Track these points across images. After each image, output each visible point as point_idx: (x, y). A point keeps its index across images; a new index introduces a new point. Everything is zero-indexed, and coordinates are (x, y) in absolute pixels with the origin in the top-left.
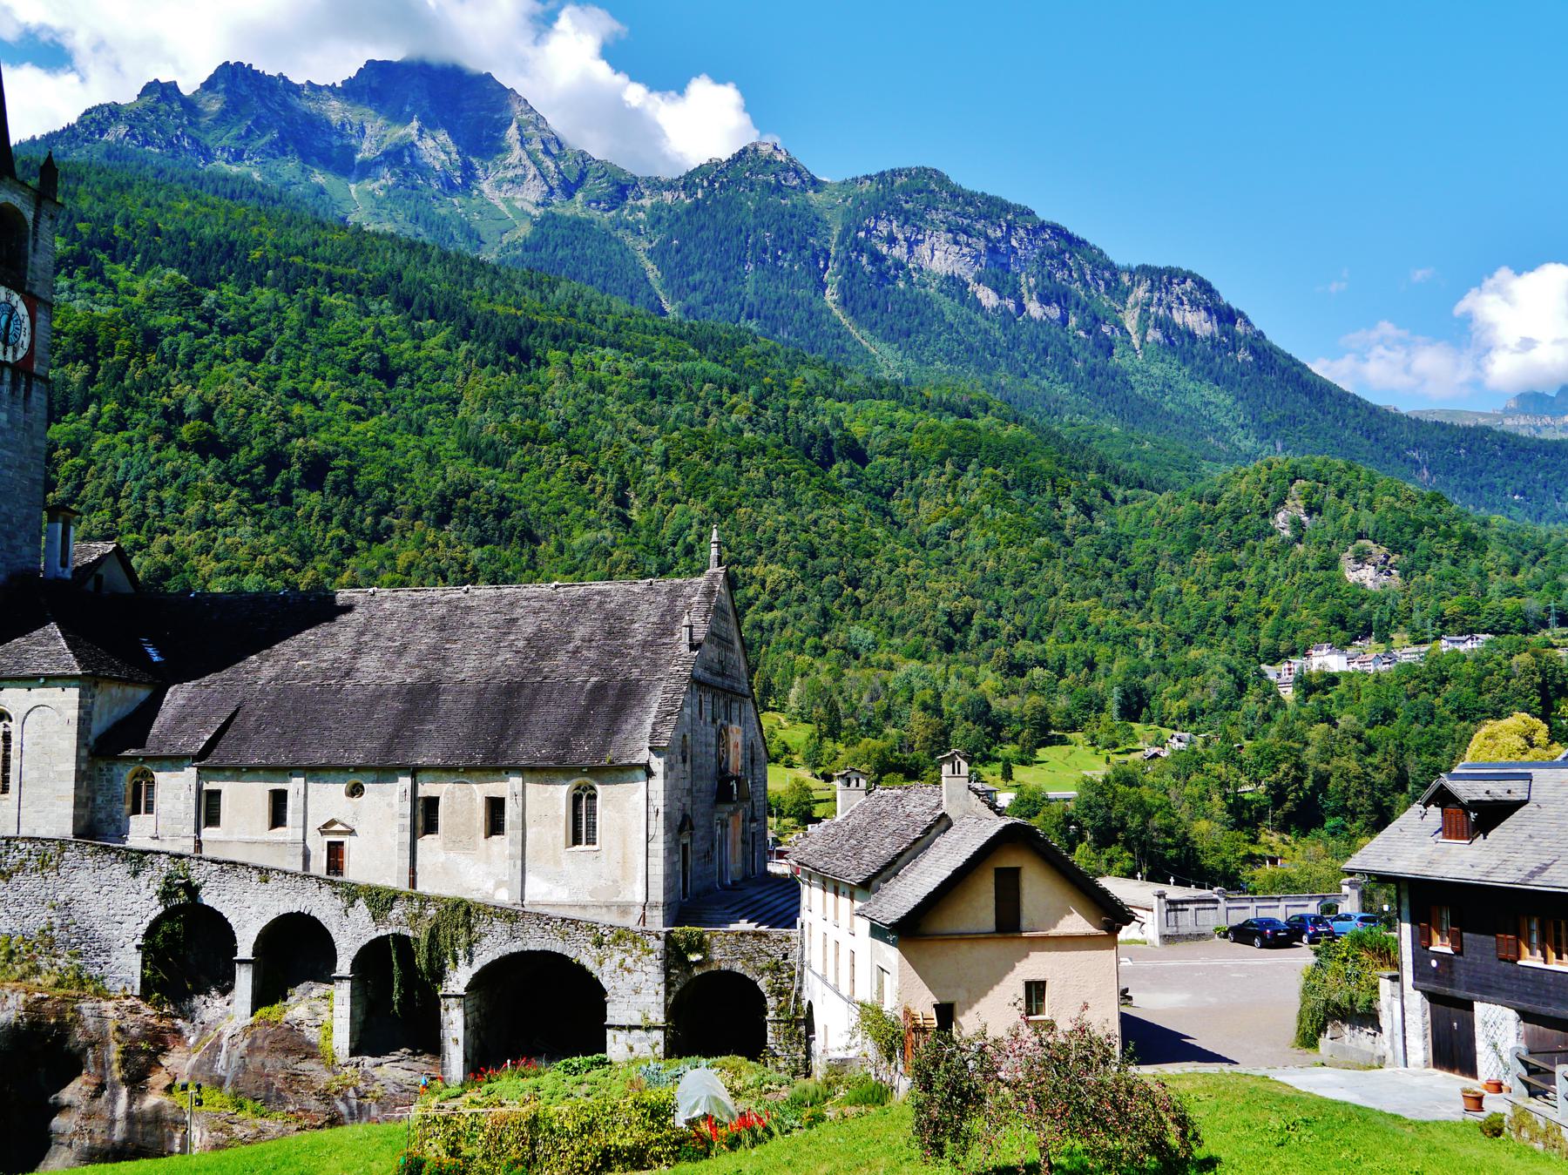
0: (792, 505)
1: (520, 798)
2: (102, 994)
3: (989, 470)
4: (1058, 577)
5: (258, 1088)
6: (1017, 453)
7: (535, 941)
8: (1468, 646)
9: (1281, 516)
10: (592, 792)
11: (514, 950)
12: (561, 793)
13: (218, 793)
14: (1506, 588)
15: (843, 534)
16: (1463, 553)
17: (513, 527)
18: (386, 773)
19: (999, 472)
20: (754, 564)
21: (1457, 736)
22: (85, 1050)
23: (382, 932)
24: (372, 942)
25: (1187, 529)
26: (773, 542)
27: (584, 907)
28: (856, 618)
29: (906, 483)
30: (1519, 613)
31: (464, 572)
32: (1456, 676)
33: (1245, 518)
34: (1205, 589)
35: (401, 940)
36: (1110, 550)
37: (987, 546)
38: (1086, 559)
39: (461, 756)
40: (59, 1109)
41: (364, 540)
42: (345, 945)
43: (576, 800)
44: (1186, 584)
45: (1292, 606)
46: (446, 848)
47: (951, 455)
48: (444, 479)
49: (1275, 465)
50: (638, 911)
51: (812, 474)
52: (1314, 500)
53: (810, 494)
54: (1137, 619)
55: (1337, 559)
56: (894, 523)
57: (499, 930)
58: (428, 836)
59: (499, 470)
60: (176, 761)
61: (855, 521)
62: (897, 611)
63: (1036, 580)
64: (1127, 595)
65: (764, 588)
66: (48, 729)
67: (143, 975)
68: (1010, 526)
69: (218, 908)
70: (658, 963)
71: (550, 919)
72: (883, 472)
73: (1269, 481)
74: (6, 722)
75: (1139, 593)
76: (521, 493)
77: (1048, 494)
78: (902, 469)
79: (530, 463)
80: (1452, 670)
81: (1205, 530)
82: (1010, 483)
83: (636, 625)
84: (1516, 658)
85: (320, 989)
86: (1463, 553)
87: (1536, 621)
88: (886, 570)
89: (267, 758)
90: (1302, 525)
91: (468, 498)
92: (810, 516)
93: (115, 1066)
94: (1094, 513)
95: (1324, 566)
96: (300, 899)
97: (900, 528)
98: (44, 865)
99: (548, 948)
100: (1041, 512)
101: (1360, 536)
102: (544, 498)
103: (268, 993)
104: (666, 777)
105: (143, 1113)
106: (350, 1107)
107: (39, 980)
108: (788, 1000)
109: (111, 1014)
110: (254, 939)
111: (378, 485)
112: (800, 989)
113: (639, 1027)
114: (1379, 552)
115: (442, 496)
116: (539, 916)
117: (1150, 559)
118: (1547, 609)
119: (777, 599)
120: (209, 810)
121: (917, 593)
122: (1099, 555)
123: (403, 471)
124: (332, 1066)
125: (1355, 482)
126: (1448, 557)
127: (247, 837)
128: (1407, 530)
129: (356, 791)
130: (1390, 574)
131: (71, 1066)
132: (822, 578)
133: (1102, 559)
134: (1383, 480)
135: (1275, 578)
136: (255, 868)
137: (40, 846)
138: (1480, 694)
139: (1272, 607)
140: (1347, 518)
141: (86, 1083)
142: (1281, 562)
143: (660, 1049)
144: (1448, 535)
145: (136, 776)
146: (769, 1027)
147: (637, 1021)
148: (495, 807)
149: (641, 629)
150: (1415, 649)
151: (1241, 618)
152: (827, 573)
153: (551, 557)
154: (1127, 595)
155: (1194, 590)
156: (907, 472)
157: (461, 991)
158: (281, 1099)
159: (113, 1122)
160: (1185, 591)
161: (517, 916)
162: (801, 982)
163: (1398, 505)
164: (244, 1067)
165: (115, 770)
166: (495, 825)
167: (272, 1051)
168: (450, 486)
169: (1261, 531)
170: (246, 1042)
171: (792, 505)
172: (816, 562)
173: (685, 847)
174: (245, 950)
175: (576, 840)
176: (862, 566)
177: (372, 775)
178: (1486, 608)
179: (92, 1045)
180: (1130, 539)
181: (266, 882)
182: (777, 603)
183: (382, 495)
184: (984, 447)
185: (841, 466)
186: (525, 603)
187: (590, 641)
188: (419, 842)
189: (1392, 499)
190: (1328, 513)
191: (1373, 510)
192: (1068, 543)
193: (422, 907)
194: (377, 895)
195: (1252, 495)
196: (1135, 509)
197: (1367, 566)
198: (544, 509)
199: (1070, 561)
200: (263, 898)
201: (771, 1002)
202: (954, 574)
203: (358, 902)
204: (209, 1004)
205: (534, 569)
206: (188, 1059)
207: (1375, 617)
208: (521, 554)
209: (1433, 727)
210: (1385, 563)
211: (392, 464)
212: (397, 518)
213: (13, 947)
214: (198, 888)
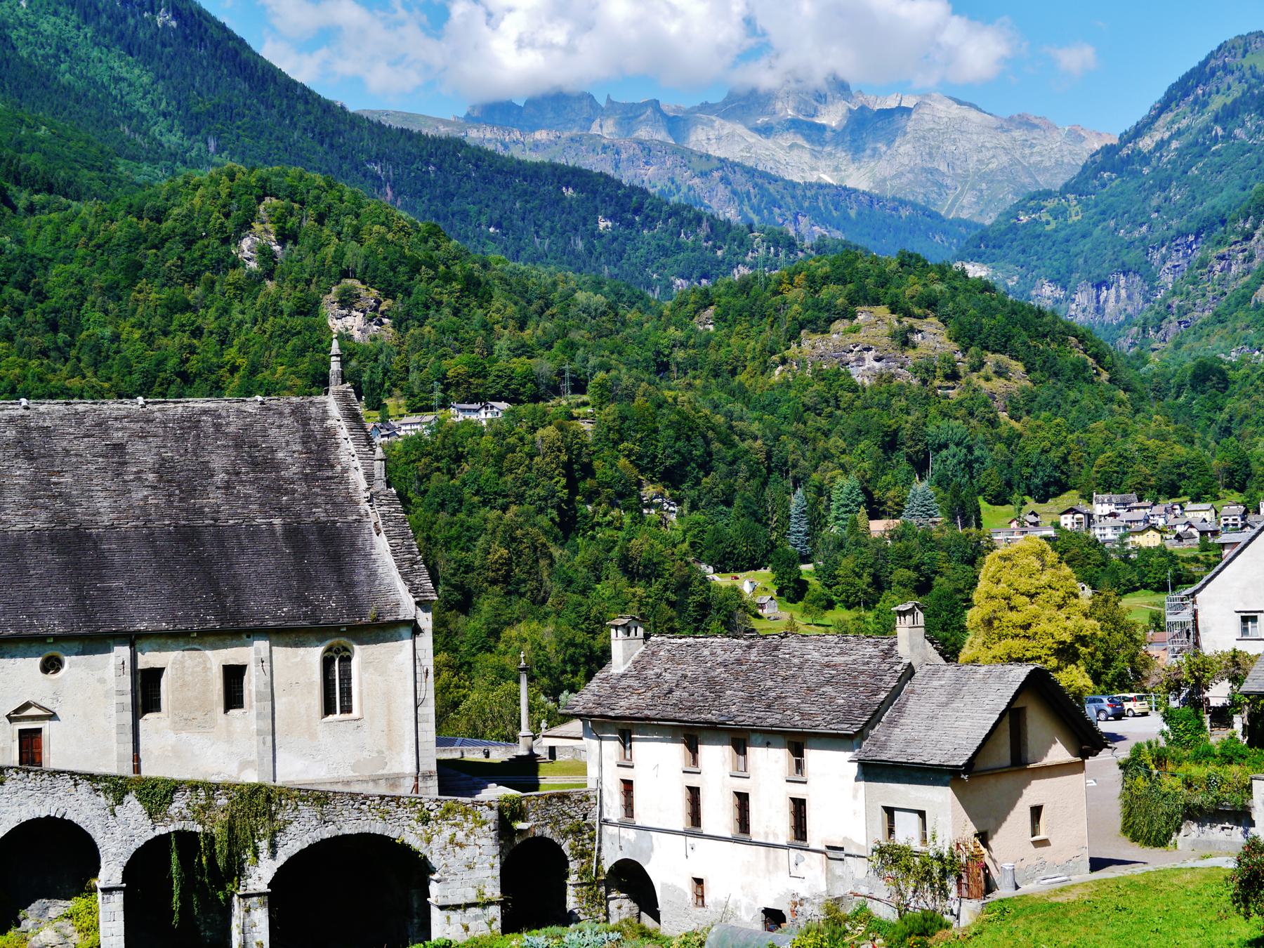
1: (267, 665)
7: (351, 825)
9: (246, 243)
10: (345, 654)
11: (327, 836)
12: (313, 655)
14: (514, 346)
16: (466, 301)
18: (95, 642)
23: (161, 830)
24: (148, 843)
25: (123, 254)
27: (348, 783)
30: (530, 377)
32: (472, 453)
33: (200, 243)
34: (151, 334)
36: (18, 276)
42: (114, 850)
43: (327, 663)
44: (125, 327)
46: (176, 729)
49: (239, 175)
50: (410, 782)
52: (289, 225)
54: (65, 373)
55: (317, 303)
57: (307, 815)
58: (148, 716)
64: (45, 340)
70: (492, 834)
71: (366, 798)
73: (231, 195)
75: (62, 337)
80: (469, 445)
81: (149, 256)
83: (280, 455)
84: (541, 432)
85: (58, 908)
87: (547, 386)
90: (273, 256)
96: (49, 800)
99: (366, 830)
101: (345, 274)
104: (435, 632)
108: (590, 861)
112: (600, 849)
113: (474, 905)
114: (369, 295)
116: (353, 796)
117: (75, 291)
118: (561, 373)
125: (338, 204)
126: (448, 305)
128: (402, 269)
129: (51, 665)
130: (381, 323)
134: (370, 206)
138: (501, 475)
139: (239, 361)
140: (330, 250)
142: (248, 303)
143: (498, 923)
144: (448, 278)
146: (571, 891)
147: (472, 897)
148: (234, 676)
149: (290, 460)
150: (415, 418)
151: (198, 374)
154: (45, 340)
155: (136, 336)
157: (263, 887)
160: (124, 336)
161: (327, 798)
162: (600, 842)
163: (390, 236)
166: (233, 698)
169: (220, 261)
175: (329, 709)
177: (76, 646)
178: (494, 370)
187: (238, 474)
188: (142, 723)
189: (383, 229)
190: (308, 242)
191: (361, 242)
193: (210, 798)
194: (153, 787)
195: (209, 214)
196: (50, 222)
197: (354, 313)
201: (574, 866)
203: (127, 798)
207: (365, 377)
209: (462, 516)
210: (375, 309)
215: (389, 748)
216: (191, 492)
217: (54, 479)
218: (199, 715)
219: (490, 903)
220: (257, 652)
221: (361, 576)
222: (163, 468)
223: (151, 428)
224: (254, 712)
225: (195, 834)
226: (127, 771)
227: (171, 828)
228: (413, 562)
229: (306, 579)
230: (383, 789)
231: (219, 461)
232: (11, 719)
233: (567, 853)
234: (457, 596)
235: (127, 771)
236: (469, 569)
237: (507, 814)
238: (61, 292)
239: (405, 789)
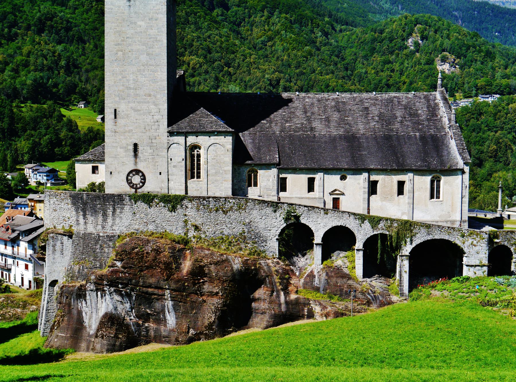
0: (199, 28)
2: (265, 257)
3: (284, 15)
4: (315, 65)
5: (336, 291)
6: (296, 7)
8: (490, 100)
9: (410, 40)
11: (429, 239)
12: (428, 179)
13: (286, 178)
15: (222, 43)
16: (486, 59)
17: (74, 36)
18: (357, 171)
19: (288, 16)
20: (184, 56)
21: (490, 138)
22: (265, 279)
23: (376, 233)
25: (369, 44)
26: (191, 45)
27: (437, 222)
28: (230, 81)
29: (246, 20)
30: (508, 86)
31: (55, 56)
32: (485, 112)
33: (395, 41)
34: (378, 71)
35: (382, 235)
36: (336, 53)
37: (284, 50)
38: (326, 57)
40: (255, 300)
41: (5, 39)
43: (432, 182)
44: (369, 69)
45: (414, 80)
47: (267, 7)
48: (40, 11)
49: (408, 17)
50: (458, 223)
51: (206, 14)
52: (425, 34)
53: (206, 23)
55: (433, 60)
56: (242, 38)
57: (423, 231)
58: (373, 196)
59: (64, 8)
60: (268, 166)
61: (227, 37)
62: (248, 78)
63: (305, 65)
64: (344, 73)
65: (189, 67)
66: (219, 153)
67: (279, 250)
68: (293, 41)
69: (307, 224)
70: (486, 243)
71: (443, 227)
72: (236, 14)
73: (406, 24)
74: (198, 150)
75: (349, 72)
76: (76, 20)
77: (309, 27)
78: (244, 13)
79: (78, 5)
80: (485, 109)
82: (293, 21)
83: (420, 112)
84: (511, 106)
85: (343, 254)
86: (486, 59)
88: (241, 60)
89: (305, 164)
90: (419, 44)
91: (52, 21)
92: (206, 34)
93: (278, 284)
94: (329, 36)
95: (427, 63)
96: (341, 220)
97: (244, 40)
98: (240, 208)
99: (443, 238)
100: (307, 35)
101: (444, 50)
102: (86, 22)
103: (325, 256)
105: (292, 301)
106: (372, 297)
107: (242, 253)
109: (271, 265)
110: (322, 236)
111: (9, 13)
114: (452, 58)
115: (40, 19)
116: (439, 226)
117: (354, 57)
119: (195, 72)
120: (282, 185)
121: (256, 70)
122: (332, 55)
123: (20, 7)
124: (358, 282)
126: (480, 61)
127: (299, 196)
129: (343, 178)
130: (455, 67)
131: (258, 283)
132: (214, 63)
133: (333, 57)
135: (407, 68)
137: (238, 201)
138: (495, 120)
140: (439, 42)
141: (267, 290)
142: (410, 61)
143: (486, 273)
144: (480, 51)
145: (249, 171)
146: (513, 264)
147: (478, 263)
148: (401, 184)
149: (422, 114)
150: (466, 100)
151: (393, 85)
152: (216, 60)
153: (92, 50)
154: (343, 73)
155: (373, 72)
156: (247, 14)
157: (407, 253)
158: (348, 294)
159: (280, 305)
160: (369, 72)
163: (460, 37)
164: (328, 283)
165: (241, 169)
166: (400, 192)
167: (337, 277)
168: (43, 15)
169: (401, 47)
170: (324, 274)
171: (198, 28)
172: (211, 55)
174: (318, 239)
175: (432, 197)
176: (231, 57)
177: (351, 172)
178: (495, 83)
179: (268, 276)
180: (345, 48)
181: (327, 214)
182: (195, 73)
183: (11, 17)
184: (281, 4)
185: (217, 11)
186: (366, 101)
187: (405, 118)
189: (457, 35)
190: (431, 39)
191: (449, 39)
192: (319, 49)
193: (392, 223)
195: (398, 31)
196: (347, 35)
197: (446, 64)
198: (87, 27)
199: (320, 57)
200: (325, 220)
202: (270, 62)
203: (365, 222)
204: (299, 260)
205: (84, 55)
206: (300, 281)
207: (449, 86)
208: (78, 48)
209: (481, 134)
210: (454, 62)
211: (14, 3)
212: (19, 30)
213: (230, 240)
214: (299, 217)
215: (452, 211)
216: (389, 123)
217: (346, 118)
218: (389, 197)
219: (484, 266)
220: (409, 177)
221: (445, 153)
222: (381, 116)
223: (377, 102)
224: (407, 197)
225: (386, 235)
226: (366, 213)
227: (379, 232)
228: (463, 149)
229: (426, 154)
230: (449, 225)
231: (399, 114)
232: (330, 194)
233: (513, 251)
234: (477, 161)
235: (366, 213)
236: (482, 152)
237: (492, 236)
238: (349, 58)
239: (457, 225)
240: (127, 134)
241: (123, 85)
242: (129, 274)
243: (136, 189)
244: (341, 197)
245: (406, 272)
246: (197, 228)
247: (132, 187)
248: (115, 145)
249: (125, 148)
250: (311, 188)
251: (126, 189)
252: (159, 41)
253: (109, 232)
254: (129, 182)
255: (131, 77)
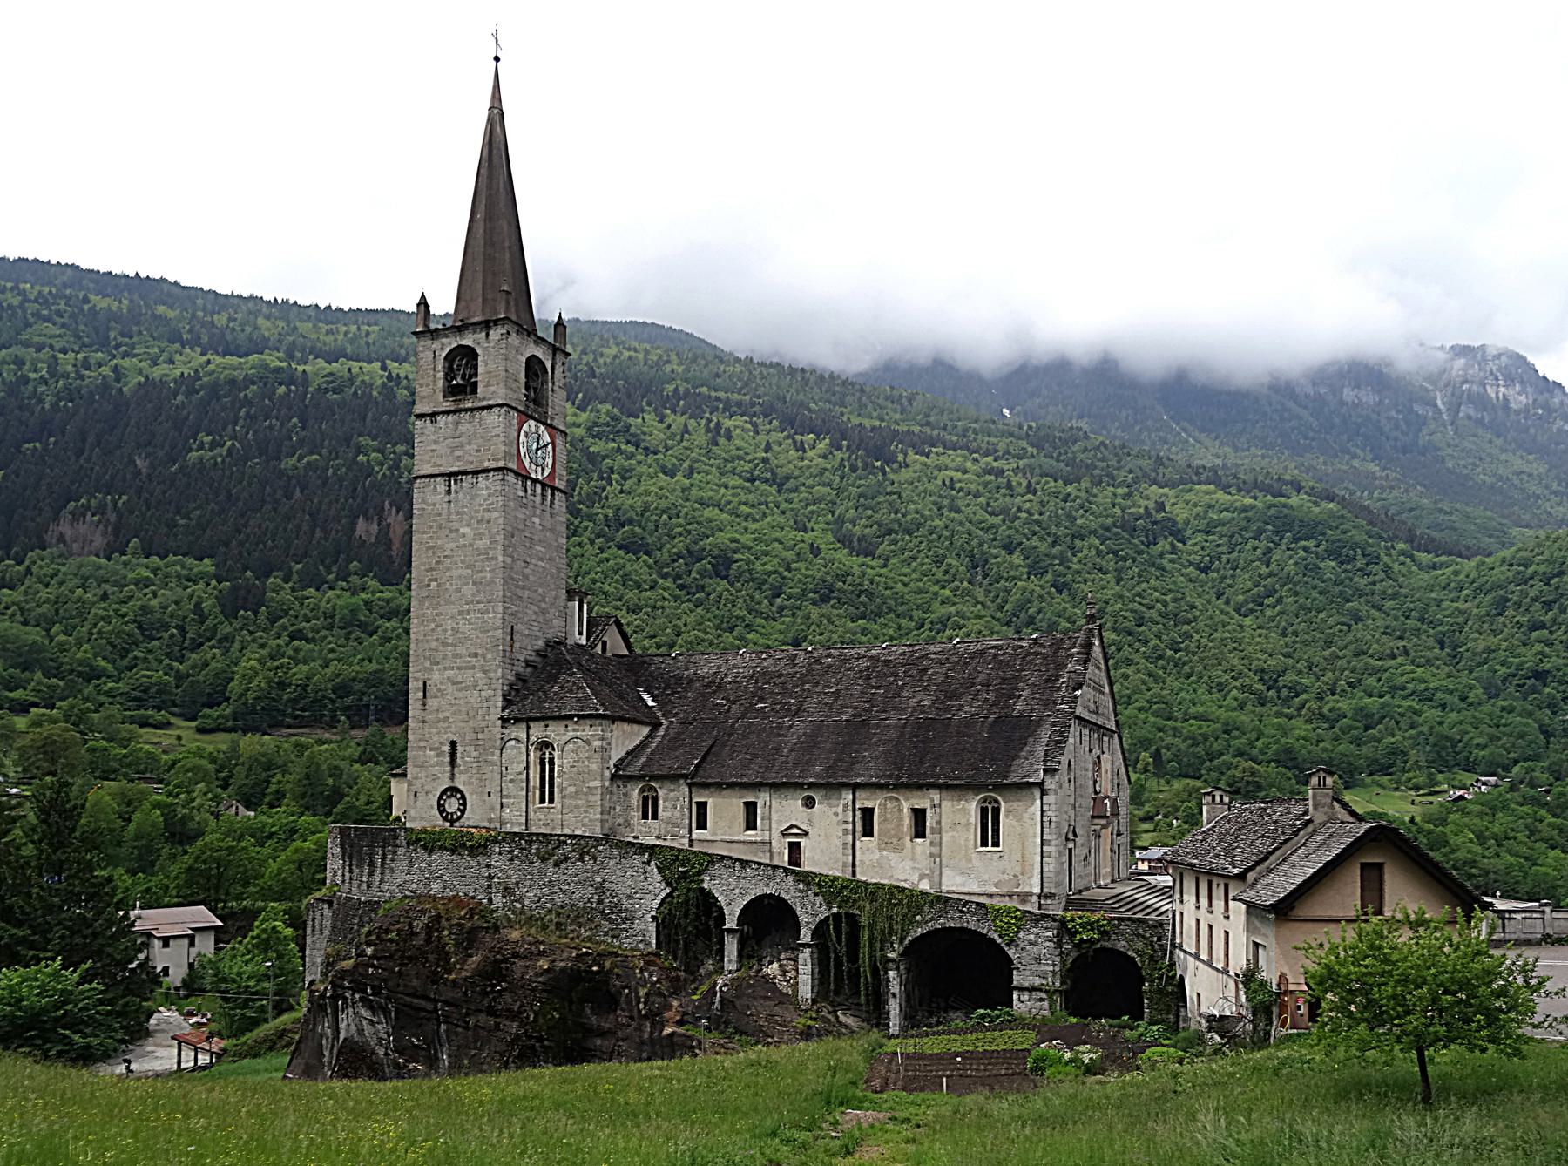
12: (972, 806)
13: (706, 803)
18: (832, 787)
27: (991, 896)
39: (890, 776)
43: (984, 812)
127: (727, 838)
129: (809, 803)
136: (737, 860)
148: (919, 815)
166: (920, 832)
173: (1070, 850)
174: (731, 923)
218: (894, 840)
224: (928, 841)
240: (441, 724)
241: (437, 640)
242: (383, 969)
243: (452, 822)
244: (803, 841)
245: (894, 995)
246: (508, 891)
247: (445, 819)
248: (423, 744)
249: (438, 749)
250: (751, 825)
251: (435, 821)
252: (492, 559)
253: (374, 896)
254: (441, 809)
255: (449, 625)
